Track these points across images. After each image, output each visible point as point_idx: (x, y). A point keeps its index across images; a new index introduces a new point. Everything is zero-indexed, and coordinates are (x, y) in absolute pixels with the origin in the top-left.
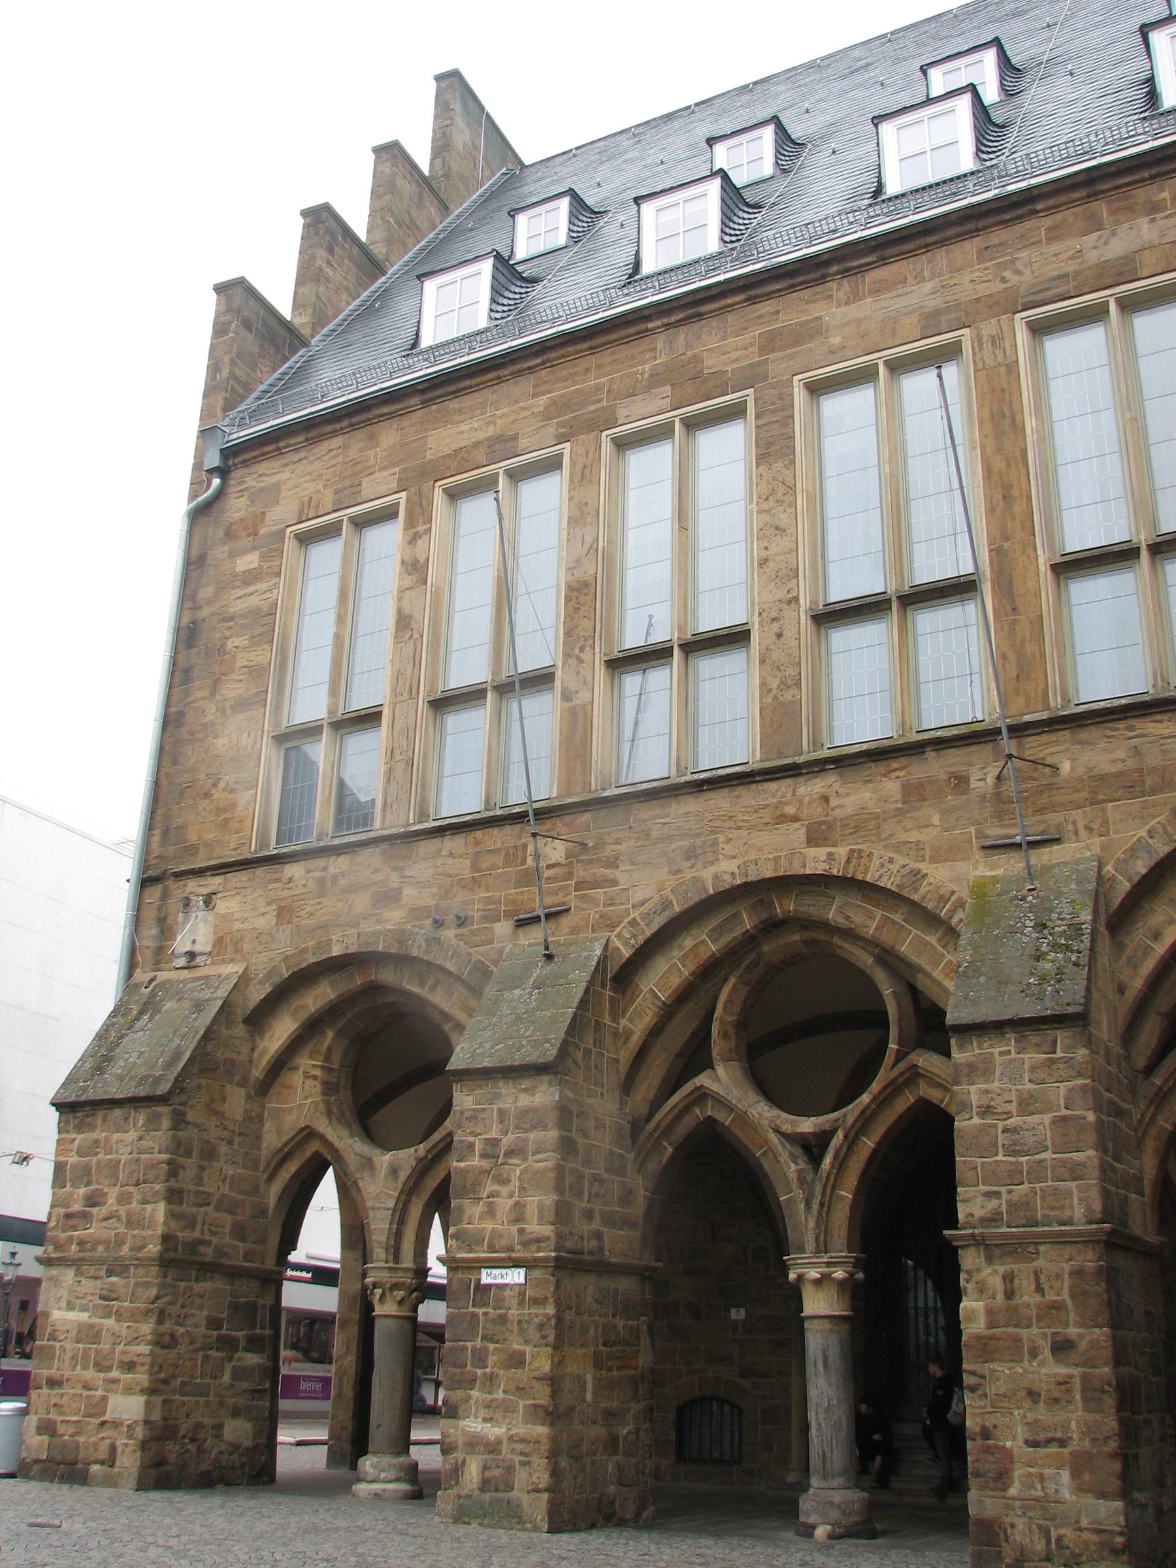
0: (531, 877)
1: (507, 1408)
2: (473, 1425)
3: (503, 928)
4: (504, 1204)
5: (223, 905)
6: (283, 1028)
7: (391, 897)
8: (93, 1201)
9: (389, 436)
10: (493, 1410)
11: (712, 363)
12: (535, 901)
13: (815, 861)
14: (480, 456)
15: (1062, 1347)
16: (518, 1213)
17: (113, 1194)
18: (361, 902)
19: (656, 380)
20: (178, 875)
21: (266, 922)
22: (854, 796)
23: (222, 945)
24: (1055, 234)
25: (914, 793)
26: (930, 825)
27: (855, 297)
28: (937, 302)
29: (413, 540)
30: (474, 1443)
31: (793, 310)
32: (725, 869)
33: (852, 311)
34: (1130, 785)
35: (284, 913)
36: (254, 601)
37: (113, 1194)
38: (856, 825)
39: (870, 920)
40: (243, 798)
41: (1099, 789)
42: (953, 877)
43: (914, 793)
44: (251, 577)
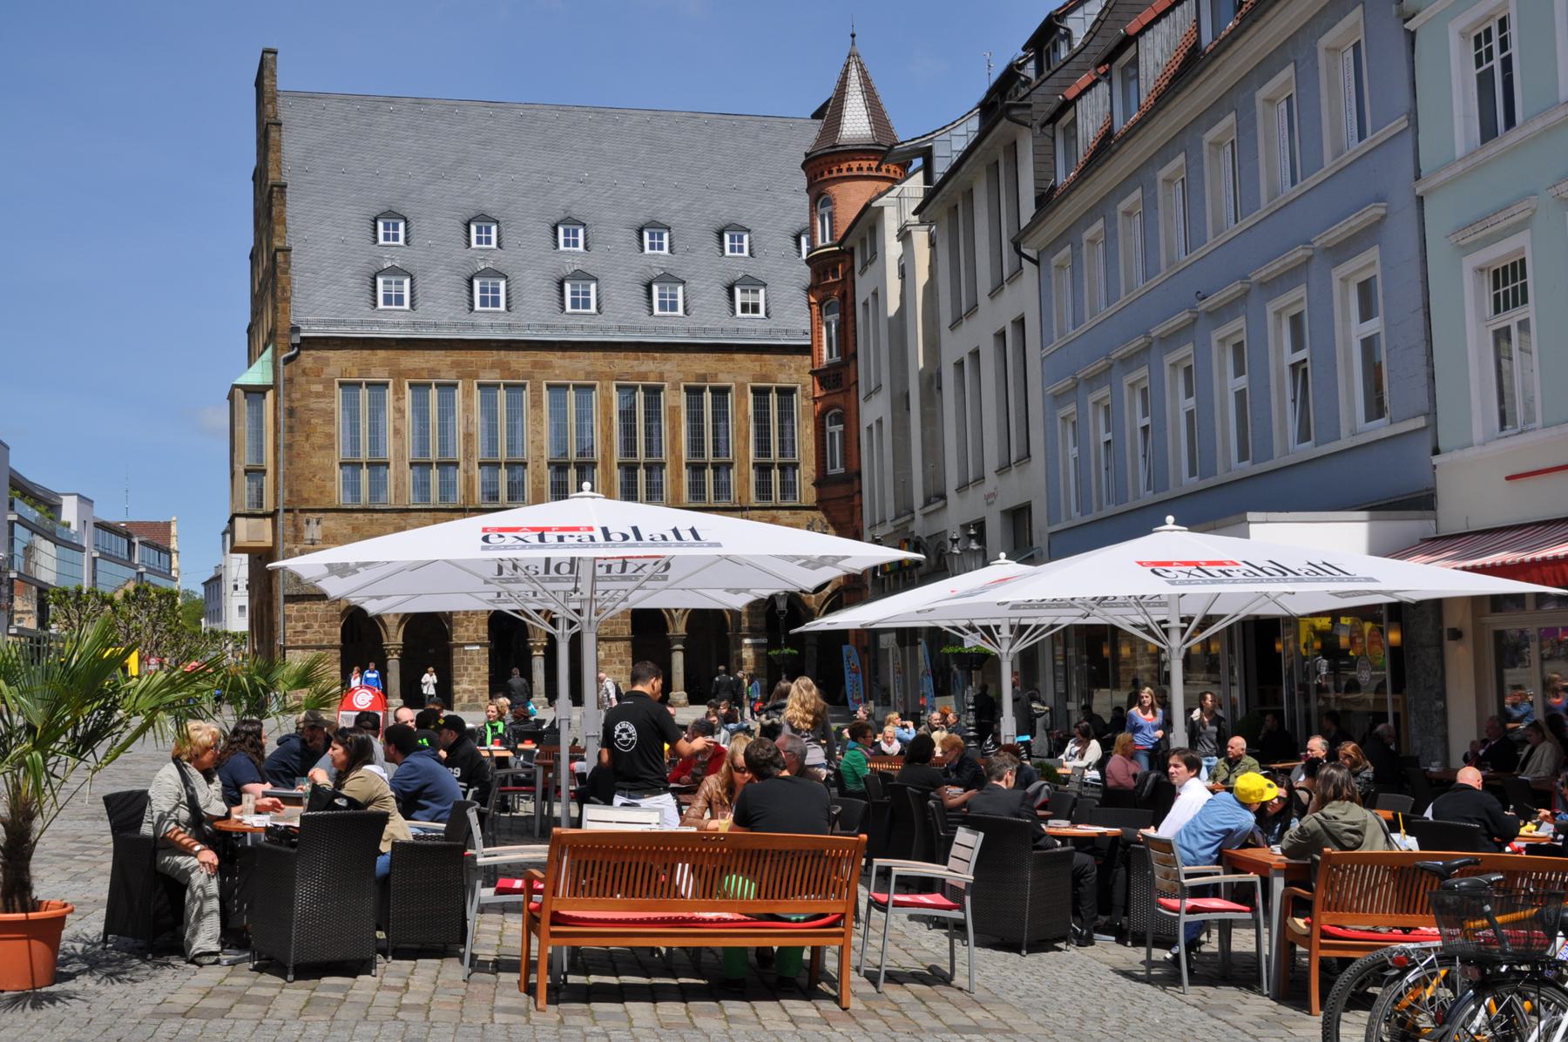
1: (475, 681)
2: (465, 686)
4: (471, 628)
5: (324, 523)
8: (306, 627)
9: (381, 354)
10: (471, 682)
11: (514, 366)
14: (425, 374)
15: (621, 662)
16: (476, 631)
17: (316, 626)
19: (493, 366)
20: (302, 511)
27: (563, 358)
28: (589, 369)
29: (398, 400)
30: (465, 691)
33: (561, 362)
36: (323, 405)
37: (316, 626)
40: (329, 484)
44: (319, 395)
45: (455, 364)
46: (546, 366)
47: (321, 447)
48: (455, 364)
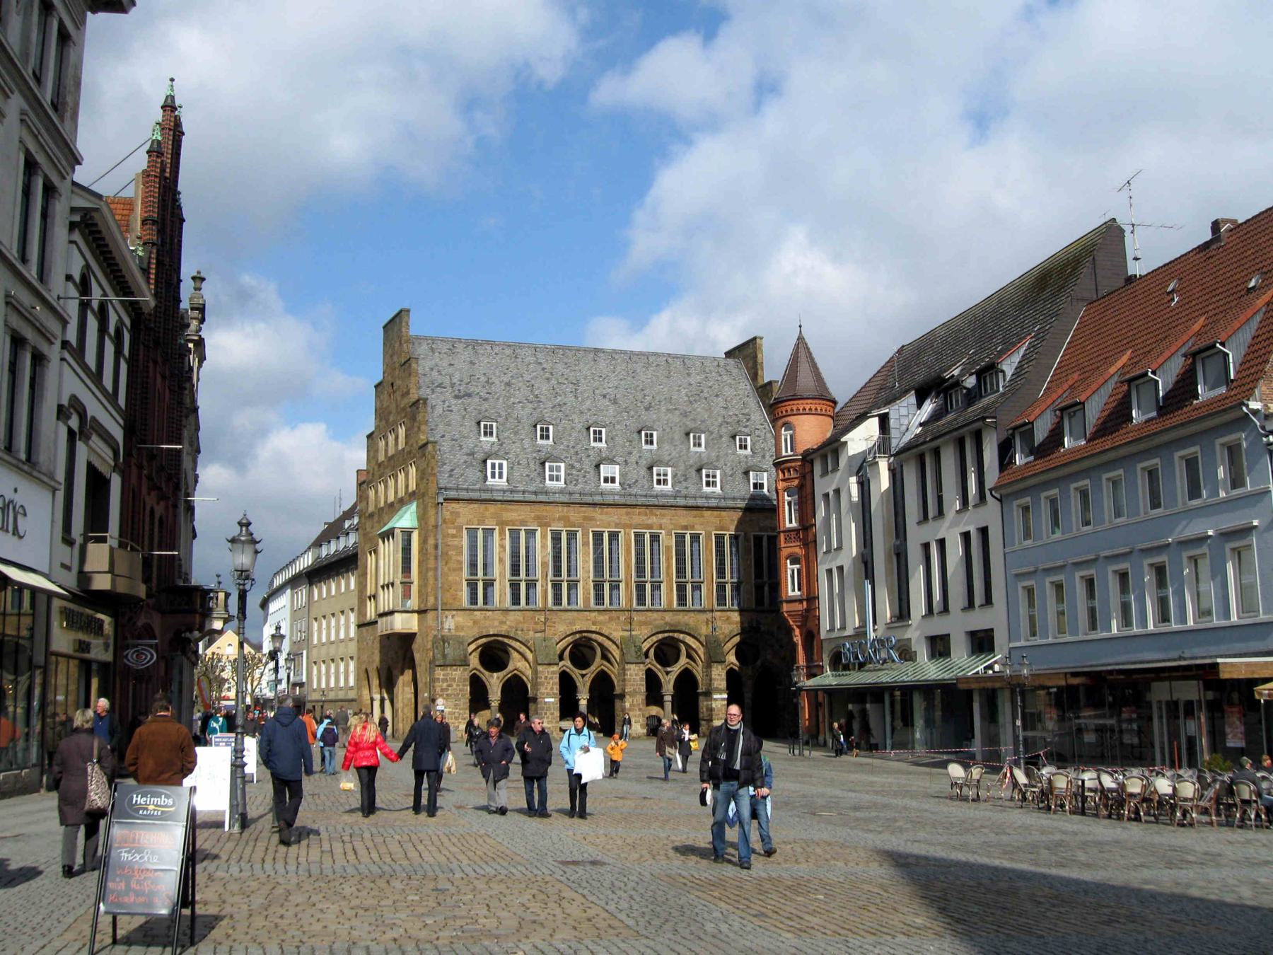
0: (536, 623)
3: (531, 633)
6: (473, 647)
7: (504, 623)
12: (538, 627)
13: (594, 628)
18: (496, 623)
19: (560, 519)
21: (471, 624)
22: (601, 618)
23: (457, 628)
24: (640, 514)
25: (611, 619)
26: (613, 625)
31: (589, 511)
32: (577, 628)
34: (645, 623)
35: (475, 622)
38: (601, 623)
39: (600, 639)
41: (641, 624)
42: (618, 634)
43: (611, 619)
45: (537, 517)
46: (591, 519)
47: (455, 570)
48: (537, 517)
